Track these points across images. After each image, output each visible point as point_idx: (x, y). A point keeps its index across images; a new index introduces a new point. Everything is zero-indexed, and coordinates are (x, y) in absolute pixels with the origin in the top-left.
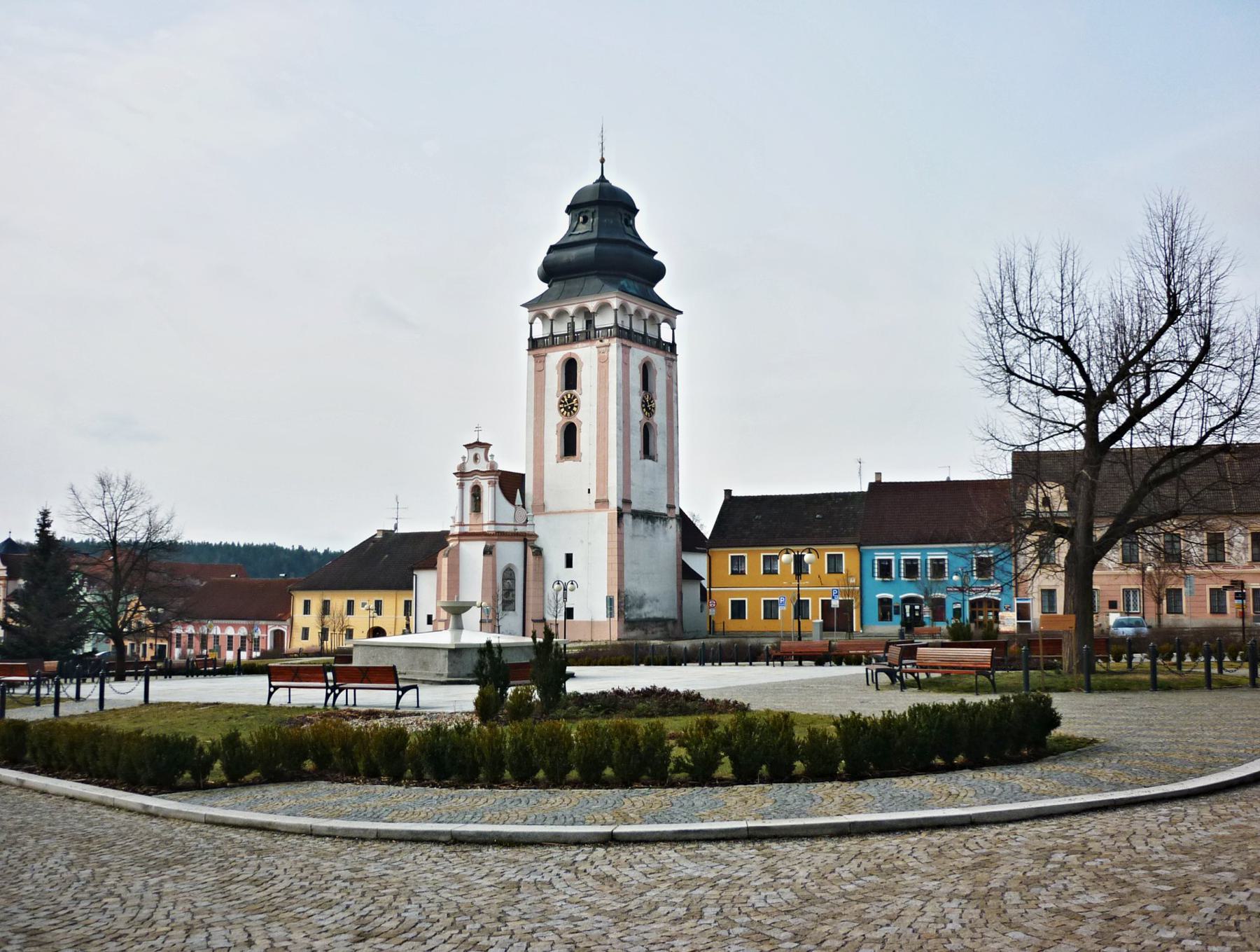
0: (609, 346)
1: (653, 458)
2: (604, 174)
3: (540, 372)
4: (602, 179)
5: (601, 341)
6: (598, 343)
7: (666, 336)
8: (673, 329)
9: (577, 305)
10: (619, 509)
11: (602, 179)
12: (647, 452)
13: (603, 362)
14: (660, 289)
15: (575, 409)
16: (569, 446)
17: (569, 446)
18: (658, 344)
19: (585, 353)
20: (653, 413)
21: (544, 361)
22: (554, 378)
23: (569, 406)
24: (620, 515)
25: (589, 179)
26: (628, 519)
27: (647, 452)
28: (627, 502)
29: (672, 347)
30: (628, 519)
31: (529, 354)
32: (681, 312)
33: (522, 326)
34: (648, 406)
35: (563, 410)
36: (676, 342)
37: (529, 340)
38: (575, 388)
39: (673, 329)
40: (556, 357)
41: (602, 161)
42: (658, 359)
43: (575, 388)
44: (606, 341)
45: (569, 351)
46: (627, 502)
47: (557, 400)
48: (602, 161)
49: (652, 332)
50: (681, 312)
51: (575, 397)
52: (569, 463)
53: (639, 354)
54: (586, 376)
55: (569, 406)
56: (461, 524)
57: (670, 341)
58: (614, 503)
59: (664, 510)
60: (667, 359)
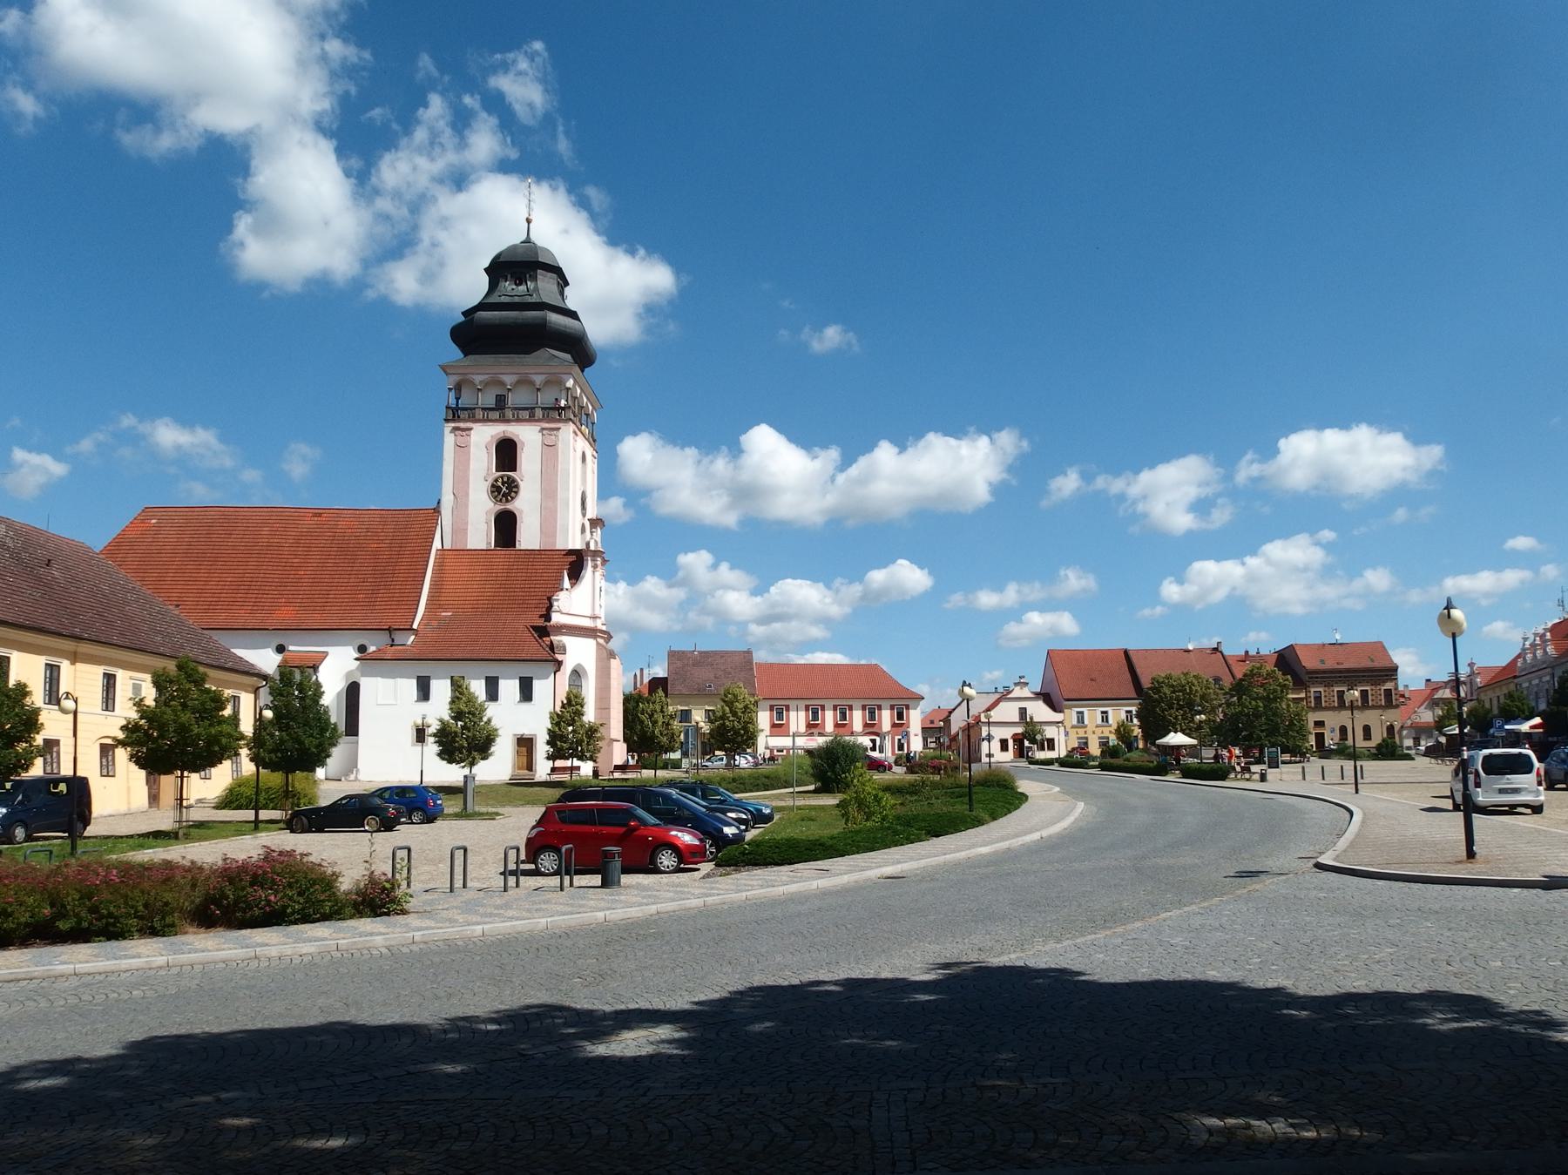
3: (462, 448)
4: (528, 241)
11: (528, 241)
13: (549, 447)
15: (513, 494)
19: (528, 436)
21: (469, 436)
23: (505, 489)
25: (517, 238)
38: (514, 470)
40: (484, 436)
41: (529, 221)
43: (514, 470)
47: (486, 486)
48: (529, 221)
51: (514, 481)
55: (505, 489)
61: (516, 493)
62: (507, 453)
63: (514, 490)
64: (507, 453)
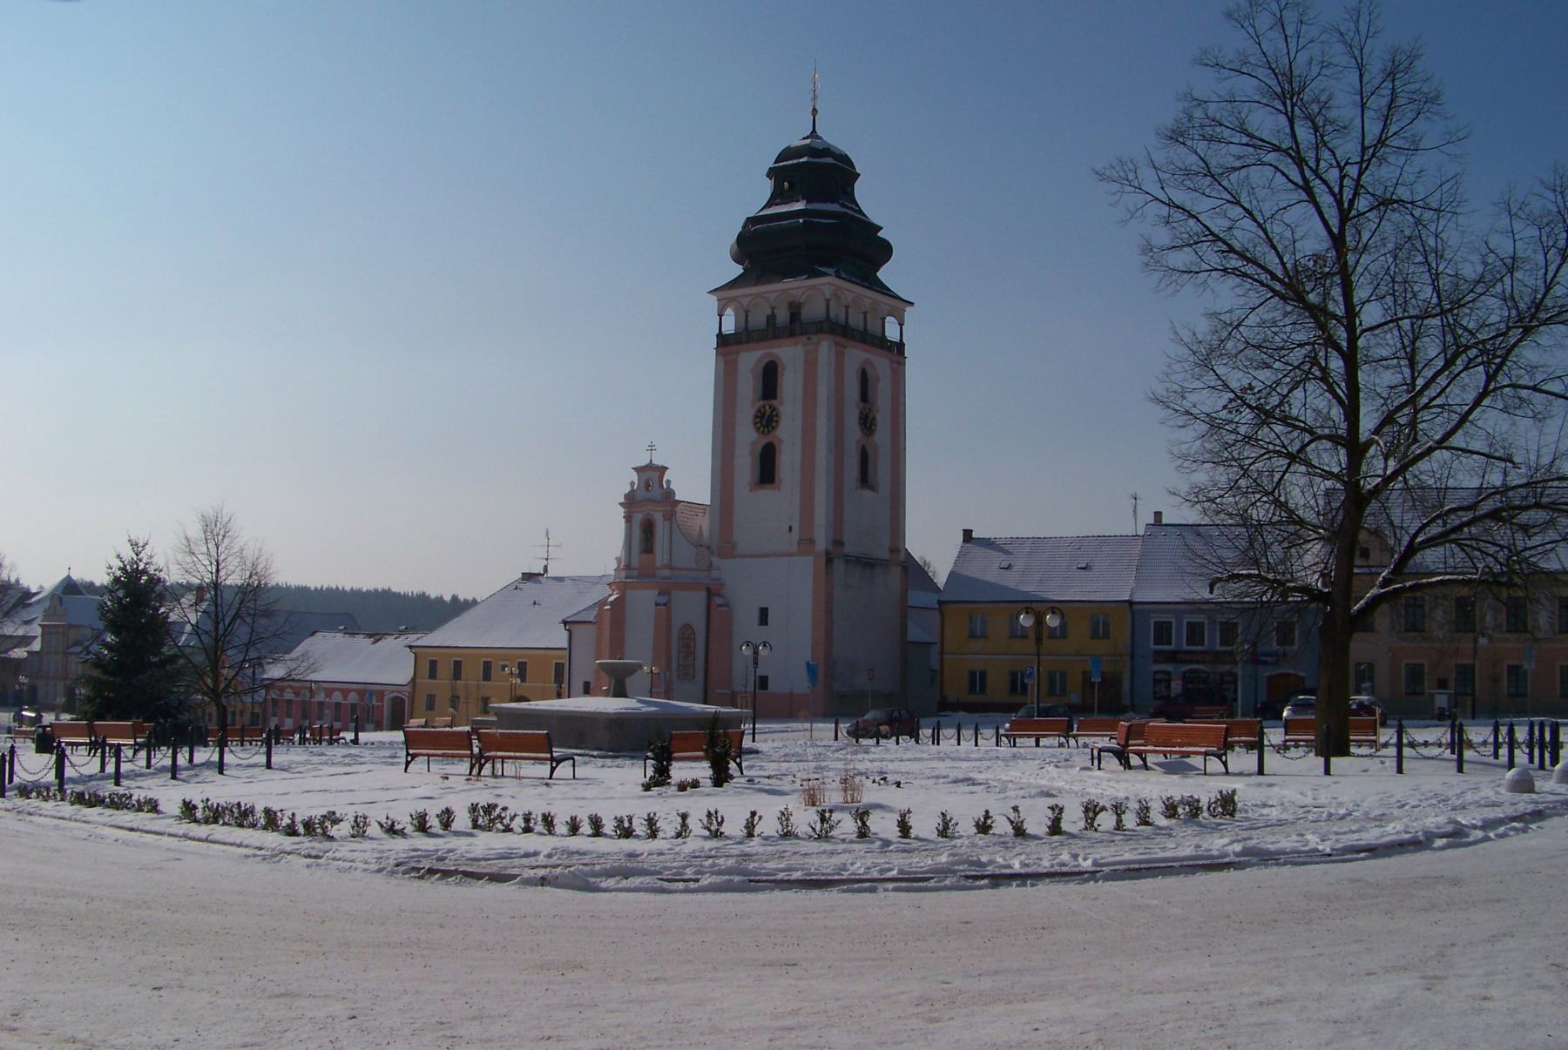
1: (872, 488)
5: (808, 339)
6: (804, 338)
7: (892, 332)
8: (901, 325)
10: (828, 553)
12: (865, 479)
13: (810, 365)
14: (885, 274)
15: (774, 424)
16: (767, 472)
17: (767, 472)
18: (882, 343)
19: (789, 354)
20: (874, 431)
22: (748, 386)
24: (829, 560)
26: (839, 566)
27: (865, 479)
28: (838, 543)
29: (900, 347)
30: (839, 566)
31: (717, 354)
32: (912, 304)
34: (867, 423)
35: (758, 425)
37: (717, 336)
38: (775, 397)
39: (901, 325)
40: (750, 360)
42: (880, 364)
43: (775, 397)
45: (768, 351)
46: (838, 543)
48: (815, 111)
49: (873, 327)
51: (774, 409)
52: (766, 493)
53: (856, 356)
54: (791, 384)
57: (896, 338)
58: (821, 543)
59: (885, 555)
60: (891, 361)
61: (777, 422)
62: (770, 379)
63: (775, 419)
64: (770, 379)
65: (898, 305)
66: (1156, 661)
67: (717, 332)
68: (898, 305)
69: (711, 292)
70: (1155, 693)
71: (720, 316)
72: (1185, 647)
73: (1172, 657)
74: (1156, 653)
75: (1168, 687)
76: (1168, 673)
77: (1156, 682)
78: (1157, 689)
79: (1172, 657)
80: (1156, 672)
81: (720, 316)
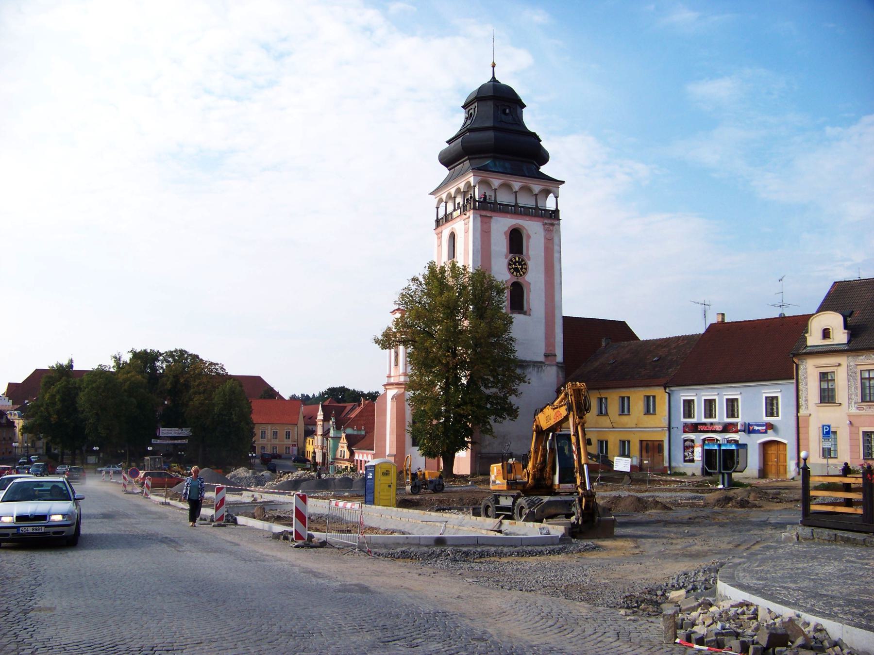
0: (469, 217)
2: (495, 76)
7: (550, 204)
8: (556, 197)
9: (542, 187)
29: (555, 214)
32: (563, 182)
33: (429, 209)
36: (559, 208)
39: (556, 197)
41: (493, 67)
44: (468, 214)
48: (493, 67)
50: (563, 182)
53: (502, 225)
56: (389, 377)
59: (541, 358)
65: (552, 184)
66: (685, 432)
67: (436, 218)
68: (552, 184)
69: (431, 194)
70: (685, 457)
71: (437, 208)
72: (704, 420)
73: (695, 428)
74: (686, 425)
75: (693, 452)
76: (692, 441)
77: (686, 448)
78: (686, 454)
79: (695, 428)
80: (685, 441)
81: (437, 208)
